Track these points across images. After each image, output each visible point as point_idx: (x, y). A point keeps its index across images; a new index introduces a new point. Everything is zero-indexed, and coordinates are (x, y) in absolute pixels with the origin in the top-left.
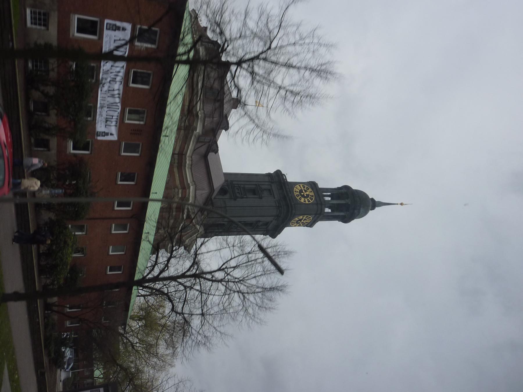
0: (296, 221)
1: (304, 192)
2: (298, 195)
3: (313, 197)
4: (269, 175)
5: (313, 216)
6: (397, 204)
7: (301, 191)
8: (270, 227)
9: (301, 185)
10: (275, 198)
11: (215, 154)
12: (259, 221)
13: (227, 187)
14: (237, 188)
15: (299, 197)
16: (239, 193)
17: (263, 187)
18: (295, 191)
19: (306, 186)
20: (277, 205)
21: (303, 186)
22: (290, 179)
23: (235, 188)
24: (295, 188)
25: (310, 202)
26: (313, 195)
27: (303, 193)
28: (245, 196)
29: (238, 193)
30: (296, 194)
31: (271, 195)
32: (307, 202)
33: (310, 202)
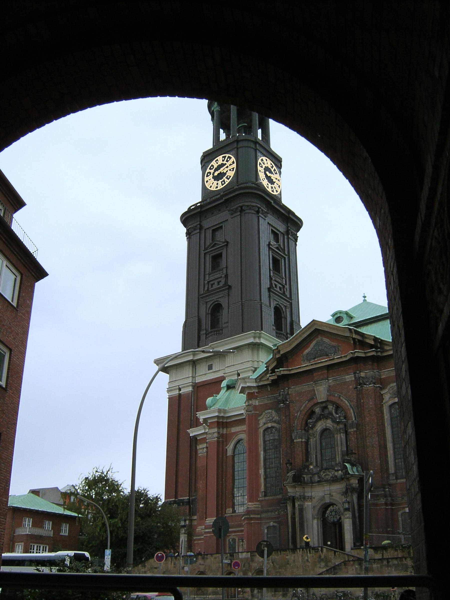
0: (270, 184)
2: (222, 182)
3: (226, 156)
4: (188, 234)
5: (259, 154)
8: (281, 227)
11: (26, 205)
12: (269, 245)
16: (219, 283)
18: (216, 188)
19: (208, 170)
21: (207, 176)
24: (212, 189)
26: (223, 157)
29: (218, 284)
30: (220, 187)
31: (221, 227)
32: (235, 166)
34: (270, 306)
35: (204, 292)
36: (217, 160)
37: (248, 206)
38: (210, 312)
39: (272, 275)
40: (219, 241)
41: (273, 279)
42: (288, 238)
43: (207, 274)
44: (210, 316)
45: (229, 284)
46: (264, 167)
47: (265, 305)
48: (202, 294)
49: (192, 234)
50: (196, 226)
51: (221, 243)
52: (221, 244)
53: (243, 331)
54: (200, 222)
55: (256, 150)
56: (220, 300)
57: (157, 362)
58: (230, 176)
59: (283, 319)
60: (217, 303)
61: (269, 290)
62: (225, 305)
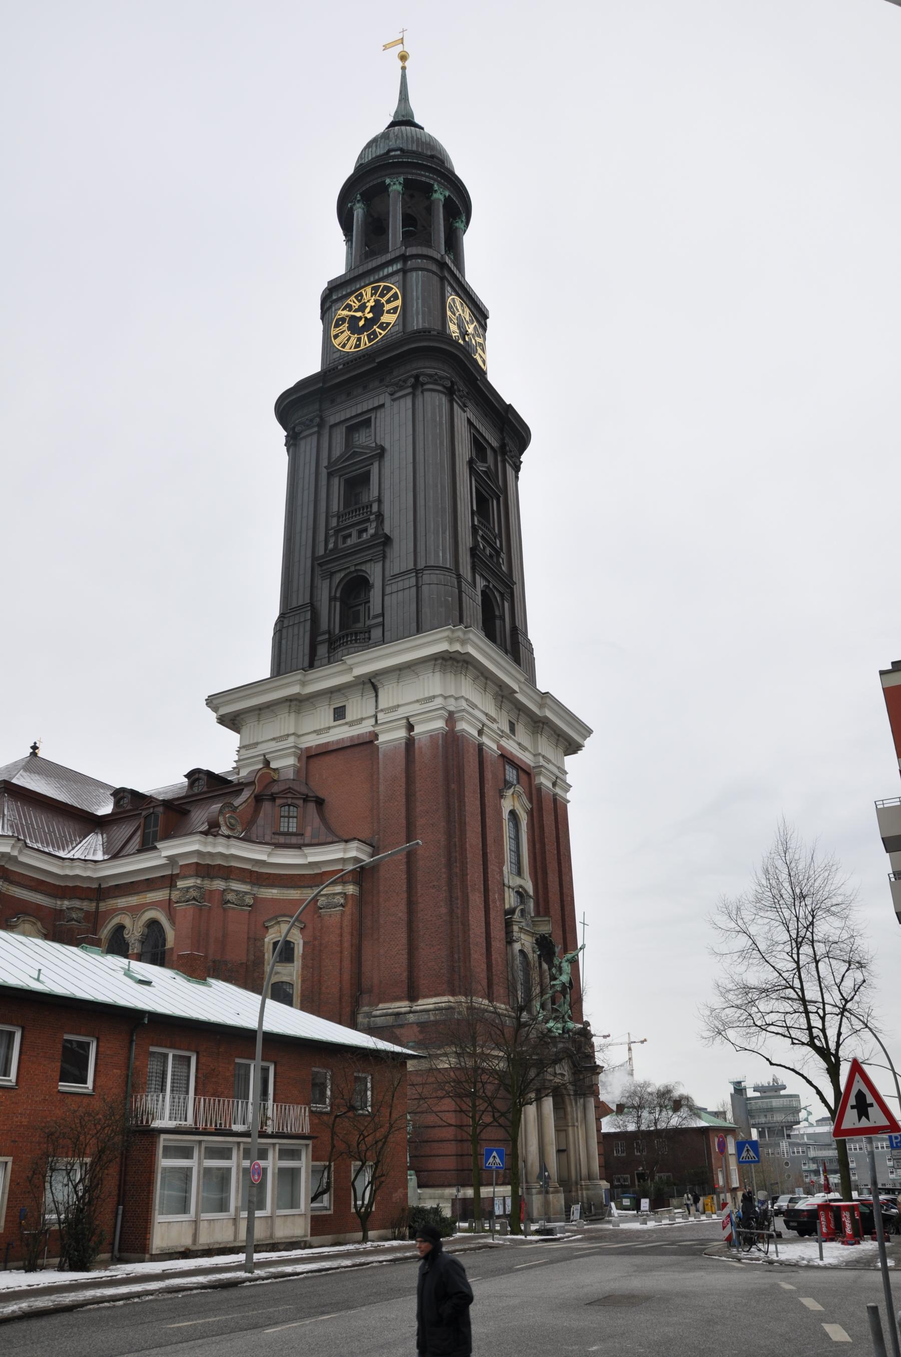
1: (359, 314)
2: (368, 336)
4: (292, 442)
6: (404, 69)
7: (354, 328)
9: (334, 332)
10: (382, 406)
12: (471, 462)
13: (338, 577)
14: (340, 540)
15: (377, 330)
16: (361, 532)
17: (338, 449)
20: (409, 390)
21: (337, 326)
22: (314, 366)
23: (340, 546)
24: (347, 349)
25: (396, 293)
26: (373, 288)
27: (360, 318)
28: (375, 508)
29: (359, 537)
31: (369, 419)
32: (399, 303)
33: (396, 293)
34: (475, 586)
35: (328, 552)
36: (361, 295)
37: (430, 376)
38: (338, 595)
39: (476, 523)
40: (363, 448)
41: (480, 532)
42: (504, 461)
43: (333, 517)
44: (338, 604)
45: (387, 530)
46: (457, 315)
47: (466, 581)
48: (322, 557)
49: (302, 436)
50: (311, 420)
51: (368, 451)
52: (366, 453)
53: (419, 630)
54: (321, 410)
55: (442, 279)
56: (363, 568)
57: (213, 702)
58: (388, 324)
59: (498, 622)
60: (355, 574)
61: (473, 551)
62: (376, 580)
